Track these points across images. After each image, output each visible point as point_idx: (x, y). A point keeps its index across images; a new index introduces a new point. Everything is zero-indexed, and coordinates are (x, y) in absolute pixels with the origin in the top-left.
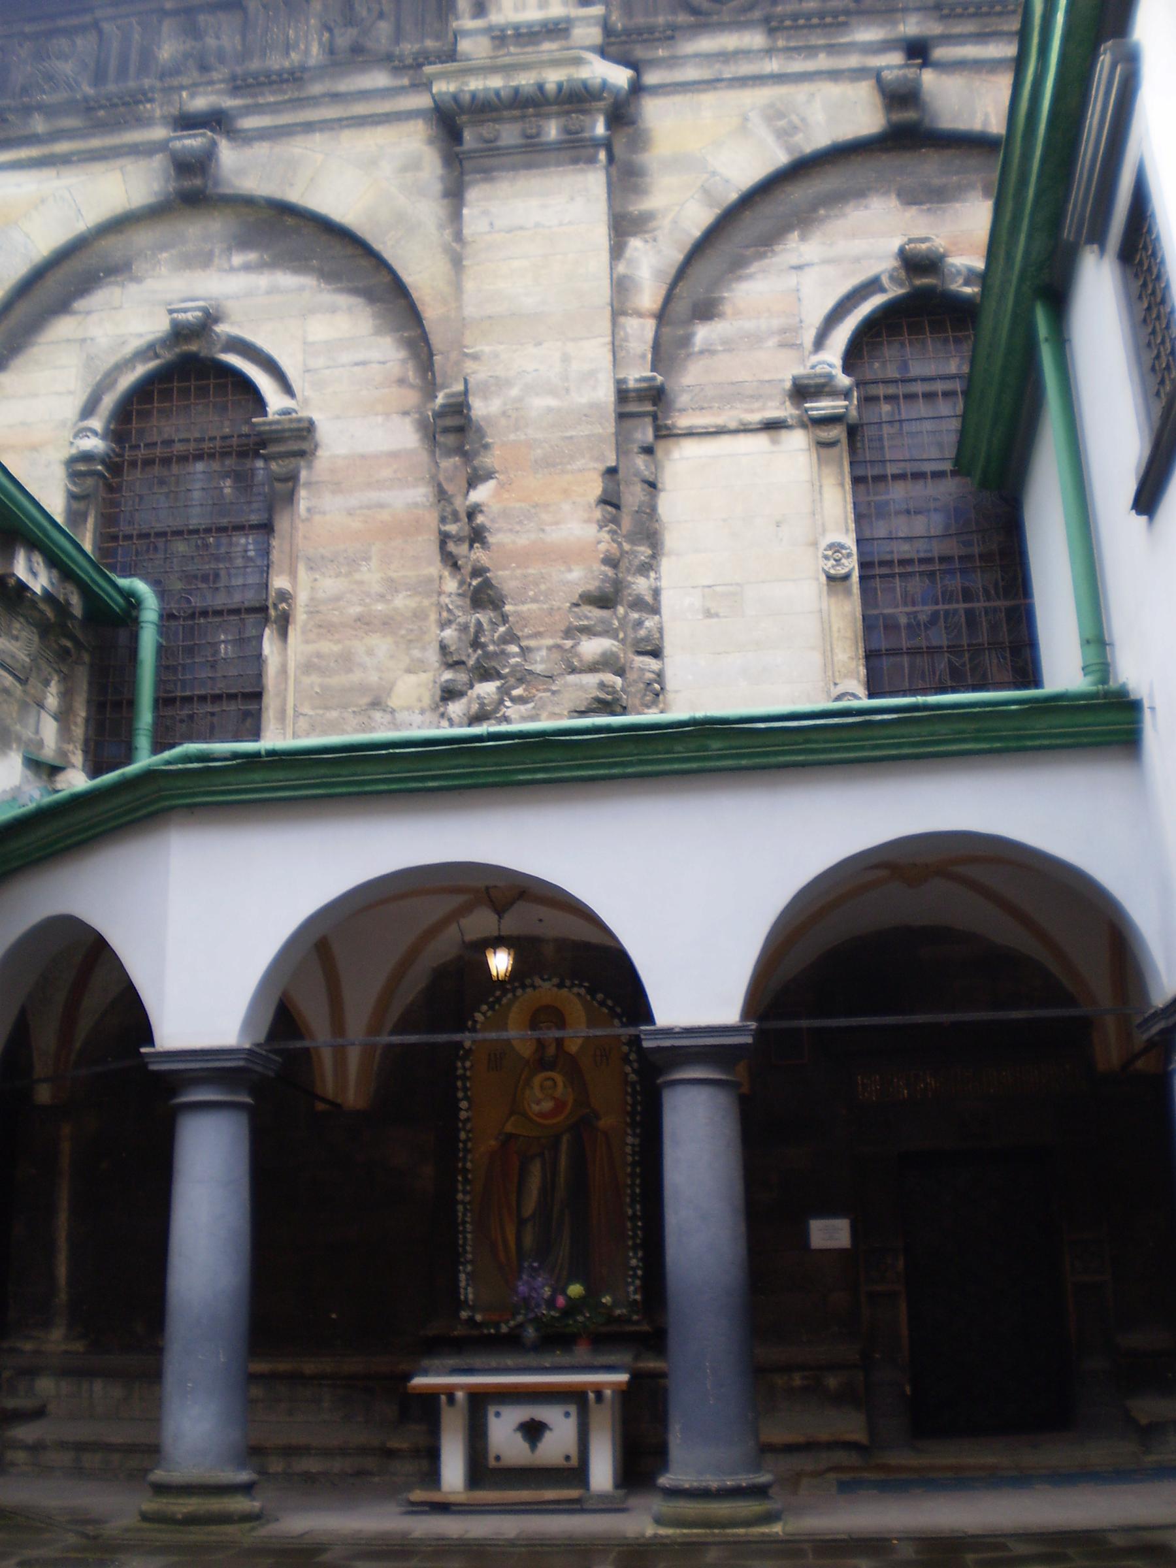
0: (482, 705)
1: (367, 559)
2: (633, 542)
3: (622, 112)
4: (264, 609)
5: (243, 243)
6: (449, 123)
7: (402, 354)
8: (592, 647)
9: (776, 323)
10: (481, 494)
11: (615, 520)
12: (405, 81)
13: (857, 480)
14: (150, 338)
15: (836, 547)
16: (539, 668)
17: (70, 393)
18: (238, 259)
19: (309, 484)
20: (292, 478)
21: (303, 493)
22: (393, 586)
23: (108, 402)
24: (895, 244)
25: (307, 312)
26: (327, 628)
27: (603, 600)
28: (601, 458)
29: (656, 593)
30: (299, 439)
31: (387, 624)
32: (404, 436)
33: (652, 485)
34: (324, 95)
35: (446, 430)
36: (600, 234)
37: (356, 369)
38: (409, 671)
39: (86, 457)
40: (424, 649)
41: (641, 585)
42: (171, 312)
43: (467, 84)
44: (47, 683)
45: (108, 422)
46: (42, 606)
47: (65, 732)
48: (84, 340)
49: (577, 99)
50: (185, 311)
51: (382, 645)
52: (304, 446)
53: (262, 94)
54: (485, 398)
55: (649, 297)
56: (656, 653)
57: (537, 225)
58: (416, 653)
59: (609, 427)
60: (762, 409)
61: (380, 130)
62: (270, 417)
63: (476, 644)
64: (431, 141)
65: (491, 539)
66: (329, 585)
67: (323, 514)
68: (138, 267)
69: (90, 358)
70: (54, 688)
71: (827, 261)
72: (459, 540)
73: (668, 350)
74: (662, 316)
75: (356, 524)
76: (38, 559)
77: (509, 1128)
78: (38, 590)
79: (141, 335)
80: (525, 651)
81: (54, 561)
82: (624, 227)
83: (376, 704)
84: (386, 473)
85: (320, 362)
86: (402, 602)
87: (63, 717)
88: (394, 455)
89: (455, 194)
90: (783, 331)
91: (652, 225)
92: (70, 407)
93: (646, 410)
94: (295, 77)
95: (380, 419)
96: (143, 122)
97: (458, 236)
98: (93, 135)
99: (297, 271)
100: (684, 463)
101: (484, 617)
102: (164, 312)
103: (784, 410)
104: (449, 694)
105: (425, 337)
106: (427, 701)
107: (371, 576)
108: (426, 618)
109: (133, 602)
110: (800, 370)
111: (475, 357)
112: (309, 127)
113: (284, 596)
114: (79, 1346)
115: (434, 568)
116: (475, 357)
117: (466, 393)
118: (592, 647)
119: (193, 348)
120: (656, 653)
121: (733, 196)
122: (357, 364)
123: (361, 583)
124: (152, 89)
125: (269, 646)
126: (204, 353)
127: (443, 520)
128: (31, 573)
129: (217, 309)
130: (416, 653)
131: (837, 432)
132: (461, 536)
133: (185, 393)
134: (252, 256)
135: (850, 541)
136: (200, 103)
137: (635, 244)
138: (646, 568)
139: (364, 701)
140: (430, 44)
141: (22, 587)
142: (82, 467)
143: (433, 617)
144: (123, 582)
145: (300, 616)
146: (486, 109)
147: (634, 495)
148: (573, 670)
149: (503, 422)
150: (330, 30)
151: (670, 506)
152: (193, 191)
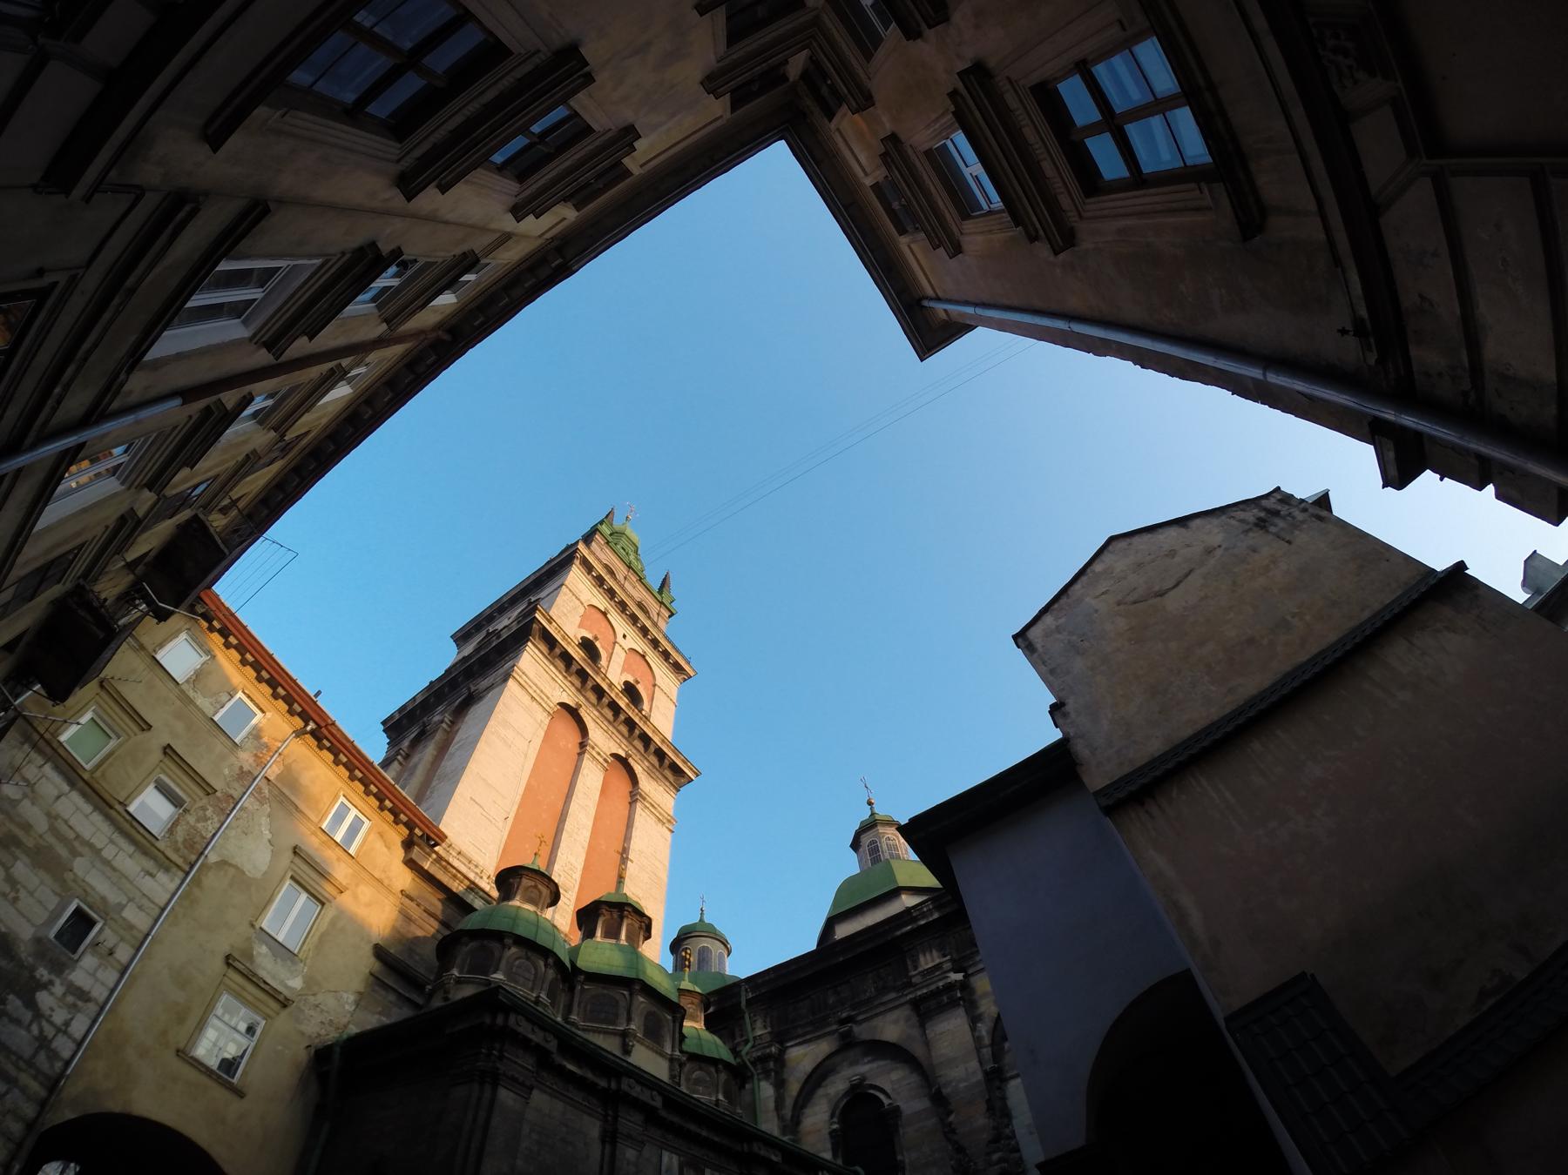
3: (965, 986)
6: (916, 1005)
10: (951, 1118)
27: (996, 1139)
30: (896, 1111)
36: (967, 1027)
41: (1007, 1131)
49: (950, 987)
55: (987, 1041)
74: (993, 1044)
82: (974, 1020)
89: (922, 1026)
92: (826, 1116)
96: (829, 1025)
112: (877, 1015)
132: (949, 1131)
138: (1007, 1126)
146: (924, 998)
151: (1009, 1103)
152: (848, 1044)
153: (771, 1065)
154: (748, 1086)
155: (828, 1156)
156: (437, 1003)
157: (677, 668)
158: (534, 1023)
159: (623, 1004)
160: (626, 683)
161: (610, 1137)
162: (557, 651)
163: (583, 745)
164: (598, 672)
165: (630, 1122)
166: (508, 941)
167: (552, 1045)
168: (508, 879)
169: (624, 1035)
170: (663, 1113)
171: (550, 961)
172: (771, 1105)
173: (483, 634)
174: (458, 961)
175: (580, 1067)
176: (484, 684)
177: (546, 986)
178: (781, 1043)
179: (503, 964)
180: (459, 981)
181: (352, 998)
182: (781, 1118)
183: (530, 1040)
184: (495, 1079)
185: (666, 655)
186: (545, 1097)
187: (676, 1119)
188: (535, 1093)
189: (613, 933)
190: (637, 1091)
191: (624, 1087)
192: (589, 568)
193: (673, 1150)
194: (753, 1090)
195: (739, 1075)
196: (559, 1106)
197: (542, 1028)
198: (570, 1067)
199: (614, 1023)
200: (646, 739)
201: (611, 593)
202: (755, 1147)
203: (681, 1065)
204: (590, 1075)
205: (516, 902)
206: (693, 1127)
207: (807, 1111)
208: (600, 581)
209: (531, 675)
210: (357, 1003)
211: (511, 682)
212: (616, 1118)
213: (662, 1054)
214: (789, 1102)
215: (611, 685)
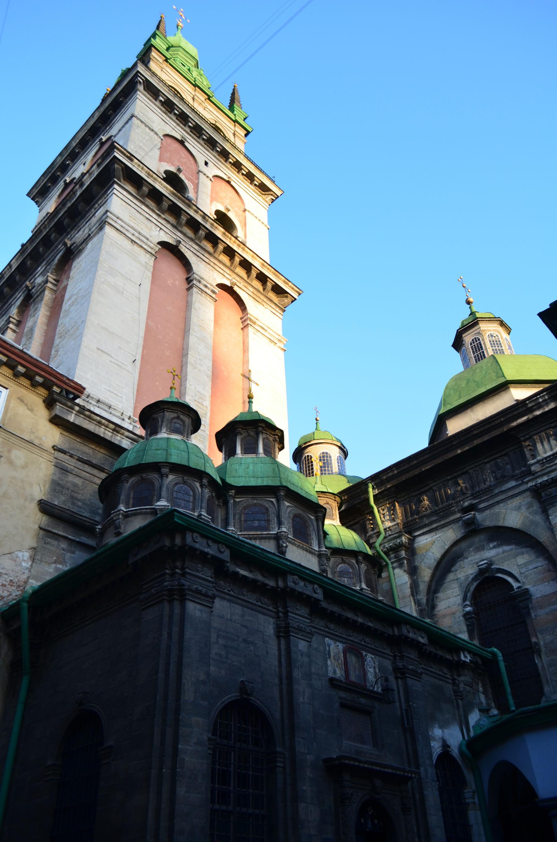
5: (491, 540)
6: (537, 492)
7: (547, 562)
12: (520, 482)
14: (475, 574)
17: (459, 595)
18: (491, 546)
20: (527, 607)
21: (532, 611)
30: (525, 594)
34: (499, 492)
37: (535, 570)
39: (468, 613)
42: (478, 566)
43: (537, 481)
44: (478, 684)
45: (471, 601)
46: (471, 664)
47: (487, 697)
50: (482, 565)
53: (482, 497)
61: (518, 498)
64: (533, 497)
66: (548, 638)
68: (465, 554)
69: (461, 584)
70: (480, 685)
76: (466, 653)
78: (469, 661)
79: (472, 574)
81: (469, 652)
84: (554, 600)
85: (523, 570)
87: (485, 693)
89: (545, 512)
92: (459, 600)
94: (489, 489)
95: (547, 583)
96: (454, 513)
97: (550, 523)
98: (441, 521)
99: (509, 545)
102: (475, 566)
105: (551, 556)
109: (494, 655)
112: (498, 503)
119: (487, 575)
122: (535, 568)
124: (452, 503)
128: (466, 658)
129: (490, 561)
134: (495, 543)
136: (466, 504)
140: (523, 469)
141: (464, 662)
142: (468, 617)
144: (489, 650)
146: (545, 486)
150: (494, 472)
152: (472, 530)
153: (403, 553)
154: (384, 575)
155: (465, 636)
156: (111, 540)
157: (263, 188)
158: (207, 538)
159: (272, 511)
160: (218, 212)
161: (284, 632)
162: (145, 189)
163: (189, 280)
164: (189, 202)
165: (299, 615)
166: (165, 470)
167: (226, 555)
168: (151, 416)
169: (277, 538)
170: (324, 605)
171: (205, 481)
172: (408, 591)
173: (61, 185)
174: (123, 497)
175: (251, 571)
176: (79, 236)
177: (204, 504)
178: (410, 533)
179: (164, 493)
180: (127, 516)
181: (27, 555)
182: (418, 603)
183: (207, 554)
184: (181, 595)
185: (250, 177)
186: (225, 603)
187: (335, 609)
188: (217, 600)
189: (251, 449)
190: (301, 586)
191: (291, 584)
192: (153, 92)
193: (336, 638)
194: (389, 576)
195: (376, 564)
196: (238, 609)
197: (215, 541)
198: (243, 572)
199: (267, 529)
200: (246, 265)
201: (183, 118)
202: (405, 630)
203: (328, 559)
204: (259, 577)
205: (163, 435)
206: (350, 615)
207: (440, 595)
208: (168, 106)
209: (126, 220)
210: (33, 559)
211: (107, 229)
212: (286, 613)
213: (311, 552)
214: (423, 587)
215: (204, 216)
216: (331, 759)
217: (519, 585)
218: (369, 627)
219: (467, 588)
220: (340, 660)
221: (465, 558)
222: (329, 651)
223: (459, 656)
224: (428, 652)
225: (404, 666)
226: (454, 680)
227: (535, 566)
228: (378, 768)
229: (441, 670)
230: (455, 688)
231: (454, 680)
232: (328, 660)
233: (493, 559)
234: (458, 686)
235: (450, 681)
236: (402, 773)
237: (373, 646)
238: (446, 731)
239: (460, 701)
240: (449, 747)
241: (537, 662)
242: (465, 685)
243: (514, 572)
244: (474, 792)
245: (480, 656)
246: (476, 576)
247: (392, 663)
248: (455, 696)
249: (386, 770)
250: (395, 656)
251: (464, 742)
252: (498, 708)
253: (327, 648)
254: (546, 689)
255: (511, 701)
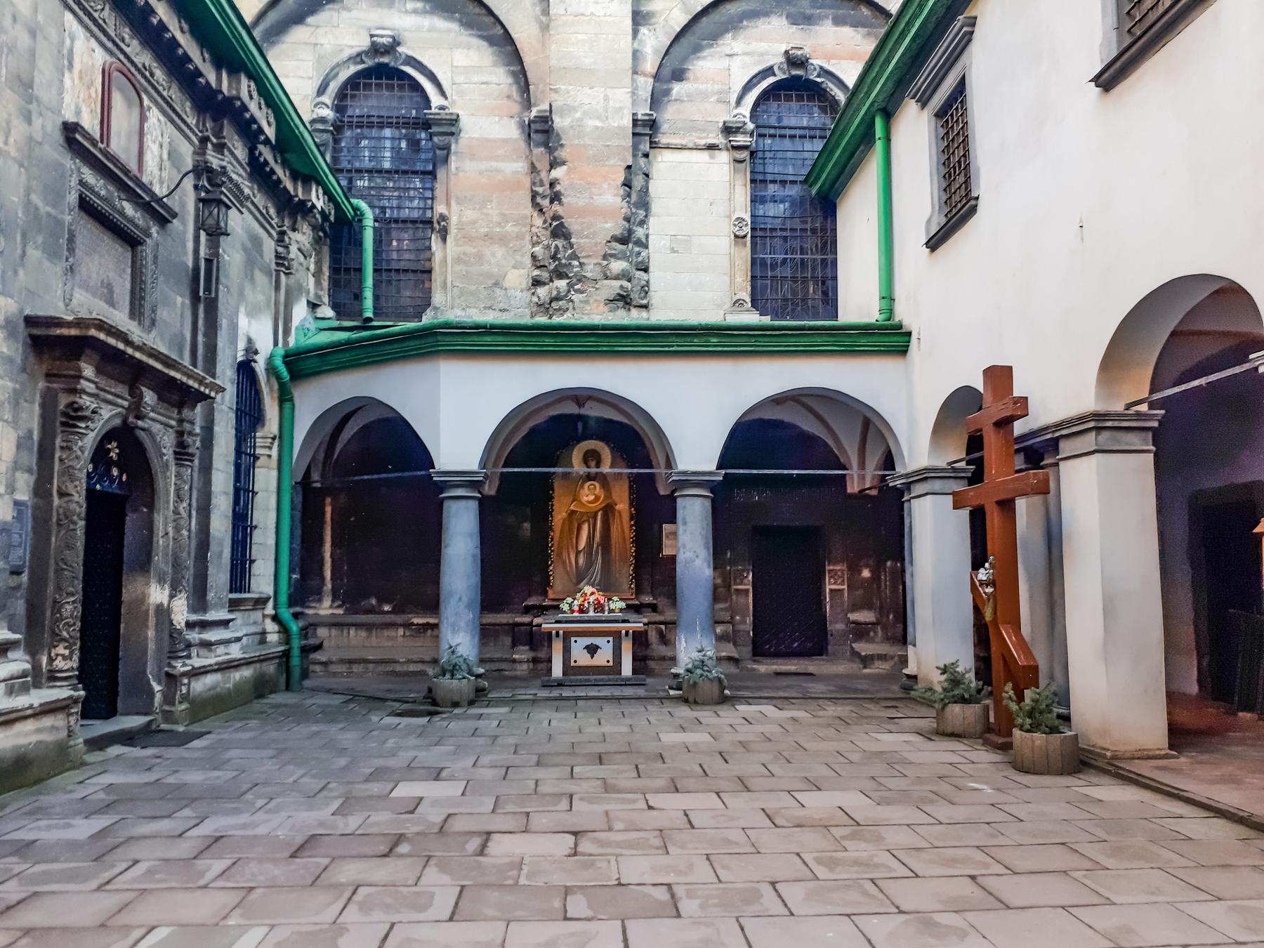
0: (559, 292)
1: (491, 201)
2: (637, 208)
4: (430, 222)
7: (510, 80)
8: (617, 266)
9: (717, 87)
10: (558, 173)
11: (629, 195)
13: (753, 181)
14: (359, 49)
15: (741, 220)
16: (589, 275)
19: (456, 153)
20: (447, 148)
21: (453, 158)
22: (505, 218)
23: (334, 86)
24: (784, 48)
25: (454, 46)
26: (470, 239)
27: (624, 240)
28: (624, 160)
29: (647, 236)
31: (502, 240)
32: (511, 131)
33: (647, 175)
35: (537, 131)
38: (514, 267)
39: (322, 120)
40: (523, 256)
42: (372, 36)
47: (318, 283)
48: (316, 44)
50: (382, 36)
51: (499, 252)
52: (453, 129)
54: (562, 117)
55: (650, 65)
56: (646, 270)
57: (592, 14)
58: (518, 258)
59: (628, 141)
60: (706, 138)
62: (433, 110)
63: (554, 257)
65: (564, 200)
66: (470, 214)
67: (463, 171)
71: (744, 54)
72: (544, 197)
73: (657, 99)
74: (656, 77)
75: (484, 180)
77: (572, 508)
79: (352, 47)
80: (581, 265)
83: (496, 284)
84: (501, 152)
86: (510, 228)
88: (505, 141)
90: (720, 93)
91: (653, 20)
93: (646, 131)
99: (447, 19)
100: (663, 162)
101: (560, 243)
103: (720, 140)
104: (537, 283)
106: (524, 285)
107: (493, 211)
108: (523, 238)
110: (727, 118)
111: (556, 91)
113: (443, 218)
114: (341, 611)
115: (528, 210)
116: (556, 91)
117: (551, 111)
118: (617, 266)
119: (385, 60)
120: (646, 270)
121: (700, 9)
123: (487, 215)
125: (435, 244)
126: (392, 64)
127: (534, 184)
128: (318, 200)
130: (518, 258)
131: (744, 155)
132: (546, 197)
133: (379, 86)
134: (420, 5)
135: (748, 218)
137: (643, 30)
139: (490, 282)
143: (528, 238)
144: (354, 201)
145: (453, 231)
147: (638, 182)
148: (607, 278)
149: (571, 132)
216: (56, 322)
217: (442, 102)
218: (174, 43)
219: (332, 69)
220: (93, 90)
221: (344, 9)
222: (71, 51)
223: (307, 191)
224: (262, 159)
225: (223, 168)
226: (282, 234)
227: (485, 79)
228: (159, 366)
229: (266, 208)
230: (280, 249)
231: (282, 234)
232: (67, 75)
233: (406, 34)
234: (287, 247)
235: (274, 234)
236: (196, 386)
237: (165, 93)
238: (253, 322)
239: (283, 276)
240: (256, 352)
241: (434, 248)
242: (299, 250)
243: (440, 76)
244: (274, 439)
245: (337, 206)
246: (359, 55)
247: (194, 153)
248: (277, 264)
249: (172, 373)
250: (204, 140)
251: (280, 351)
252: (335, 306)
253: (68, 42)
254: (438, 298)
255: (368, 302)
